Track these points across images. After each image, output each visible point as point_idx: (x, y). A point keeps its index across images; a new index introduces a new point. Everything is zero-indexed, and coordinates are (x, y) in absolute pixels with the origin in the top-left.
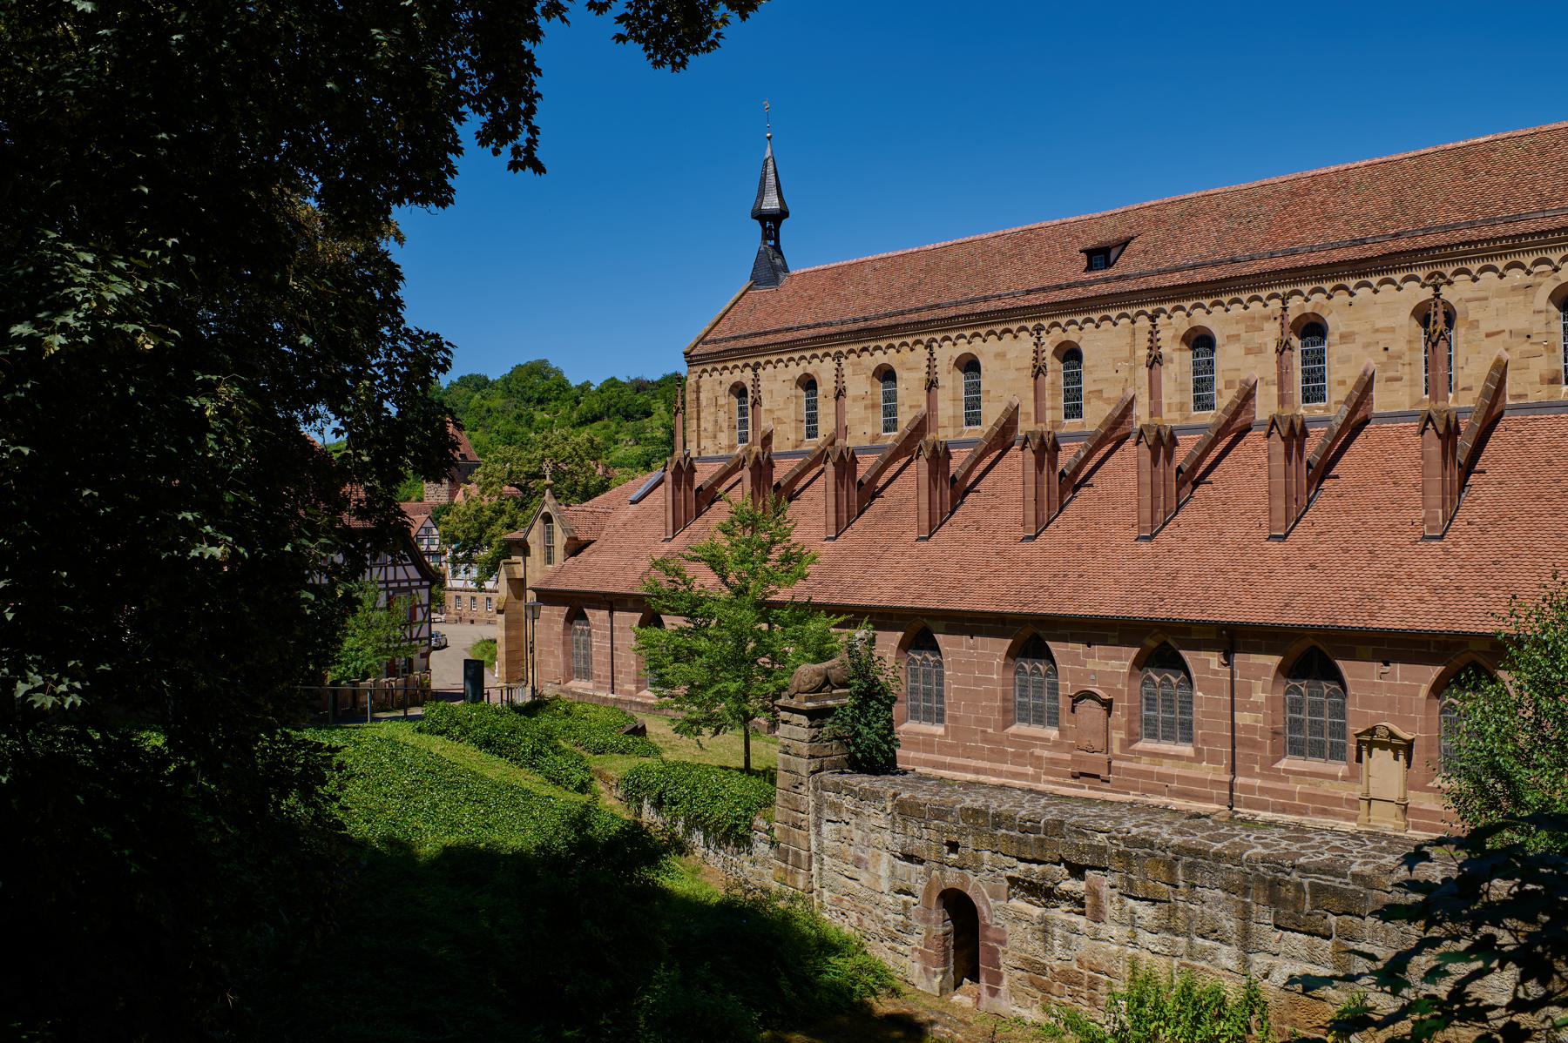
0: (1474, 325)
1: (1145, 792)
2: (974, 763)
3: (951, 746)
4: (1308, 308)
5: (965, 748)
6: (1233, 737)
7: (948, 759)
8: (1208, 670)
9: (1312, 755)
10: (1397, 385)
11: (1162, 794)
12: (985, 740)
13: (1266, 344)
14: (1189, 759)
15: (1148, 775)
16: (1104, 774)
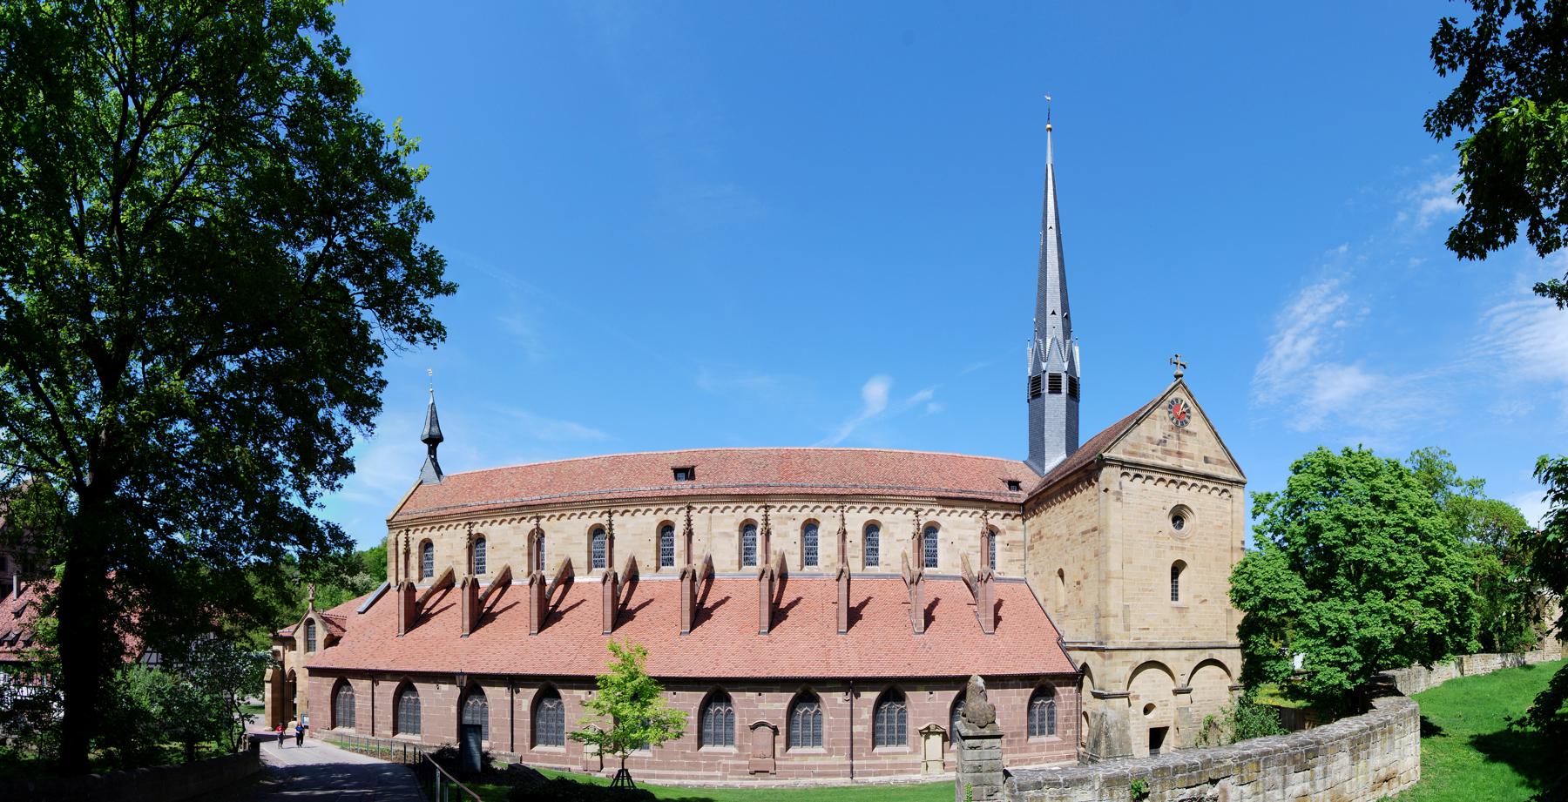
0: (892, 535)
1: (798, 776)
2: (676, 773)
3: (658, 764)
4: (812, 516)
5: (669, 763)
6: (852, 740)
7: (656, 772)
8: (836, 704)
9: (888, 743)
11: (809, 776)
12: (685, 756)
14: (824, 755)
15: (801, 767)
16: (772, 771)
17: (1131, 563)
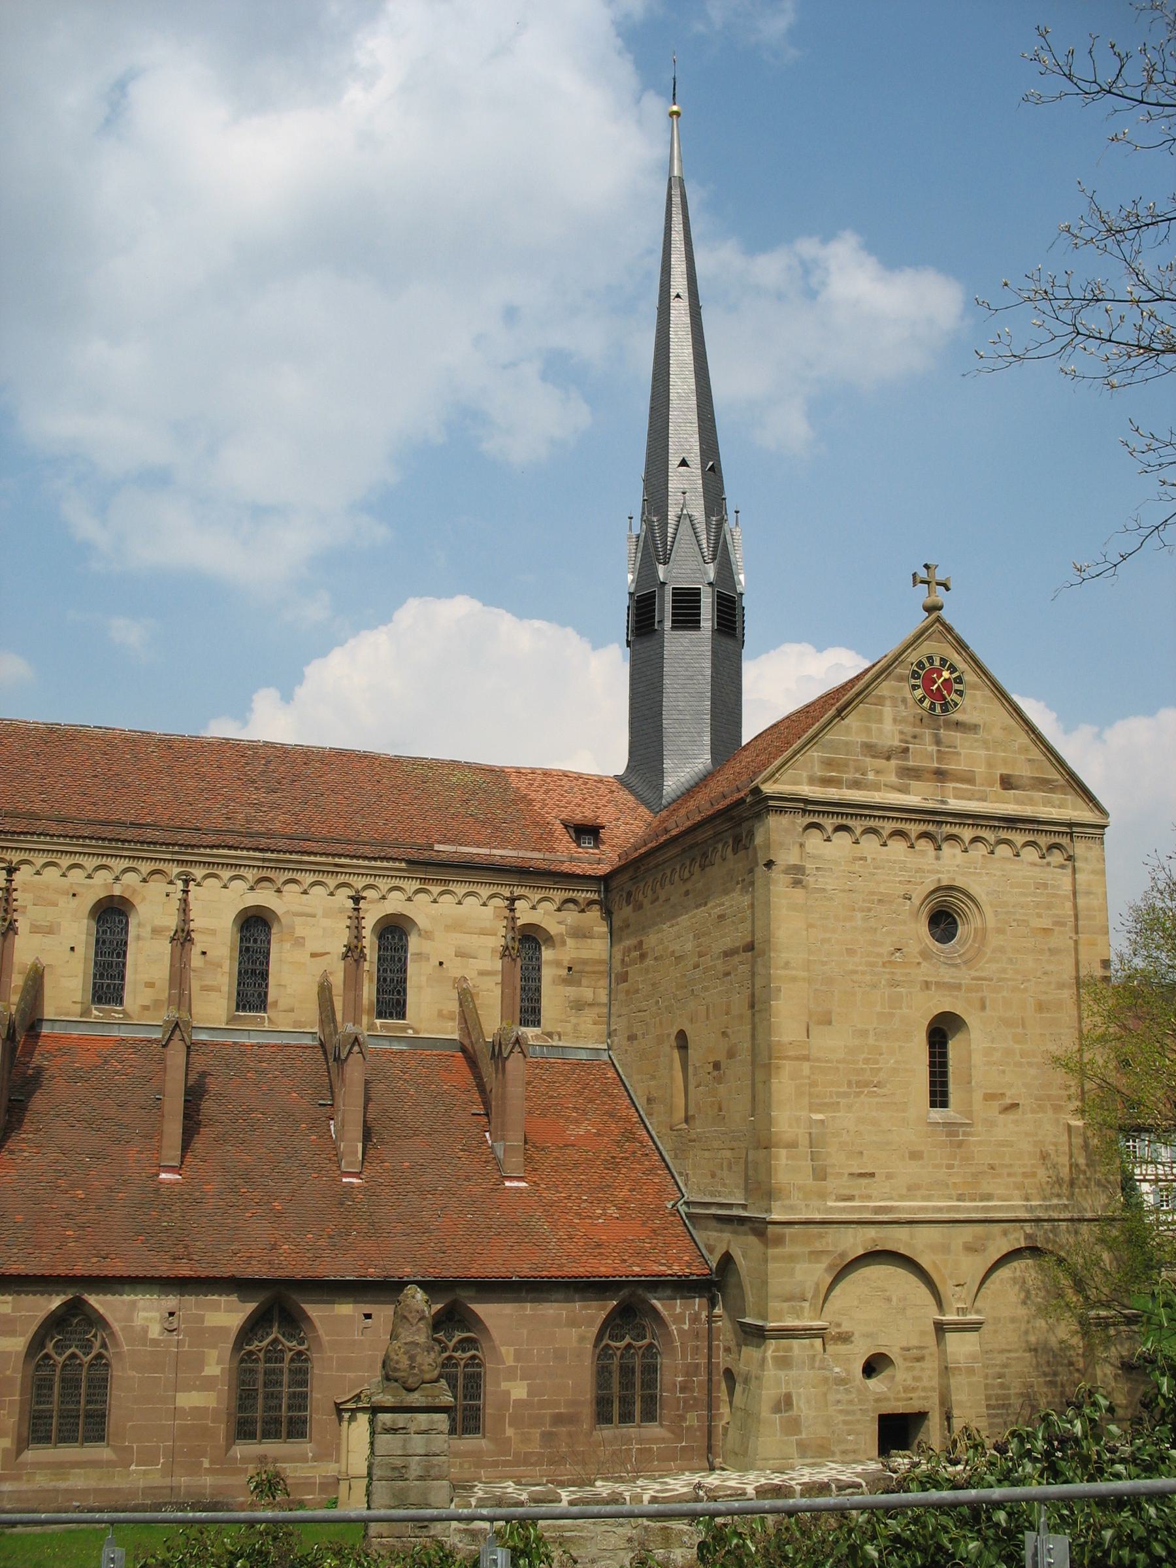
0: (299, 942)
10: (213, 995)
13: (59, 924)
17: (830, 1023)
